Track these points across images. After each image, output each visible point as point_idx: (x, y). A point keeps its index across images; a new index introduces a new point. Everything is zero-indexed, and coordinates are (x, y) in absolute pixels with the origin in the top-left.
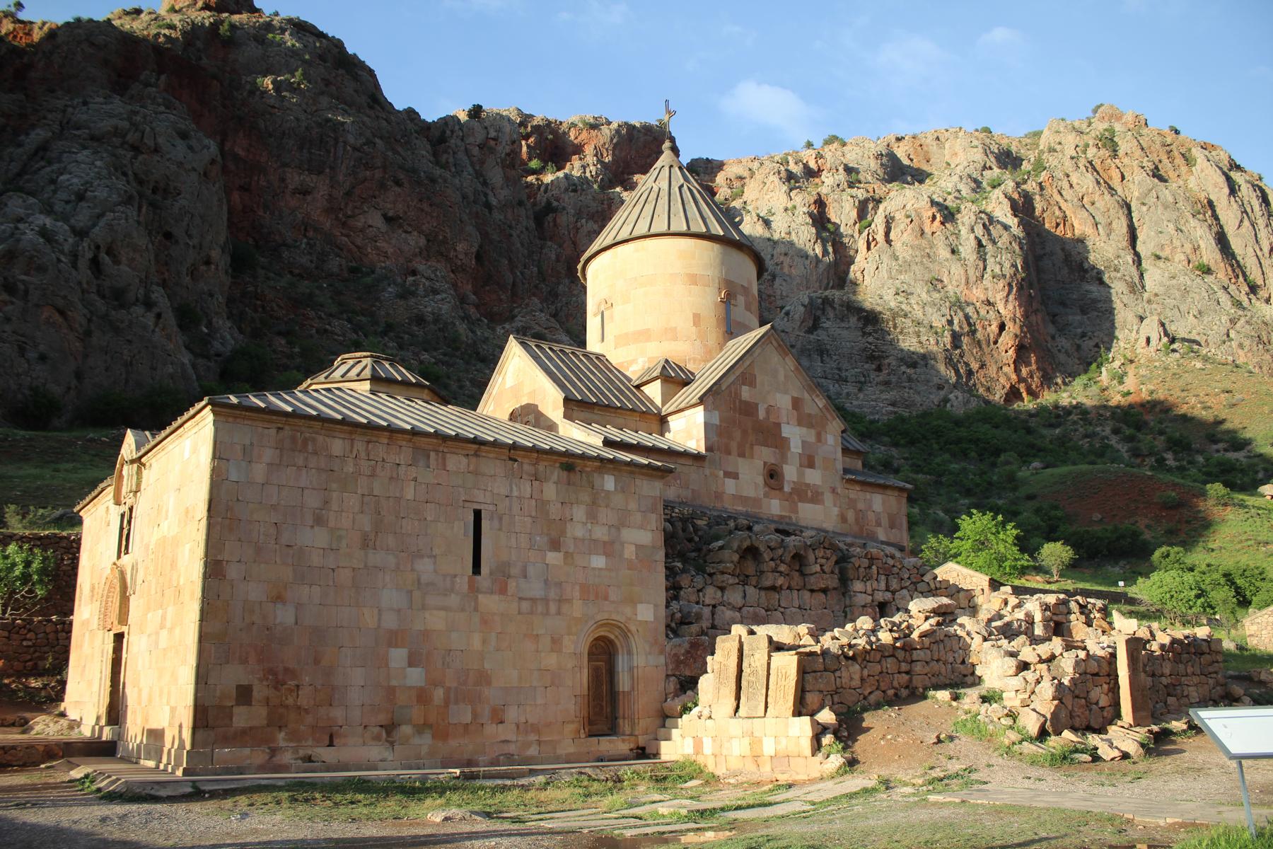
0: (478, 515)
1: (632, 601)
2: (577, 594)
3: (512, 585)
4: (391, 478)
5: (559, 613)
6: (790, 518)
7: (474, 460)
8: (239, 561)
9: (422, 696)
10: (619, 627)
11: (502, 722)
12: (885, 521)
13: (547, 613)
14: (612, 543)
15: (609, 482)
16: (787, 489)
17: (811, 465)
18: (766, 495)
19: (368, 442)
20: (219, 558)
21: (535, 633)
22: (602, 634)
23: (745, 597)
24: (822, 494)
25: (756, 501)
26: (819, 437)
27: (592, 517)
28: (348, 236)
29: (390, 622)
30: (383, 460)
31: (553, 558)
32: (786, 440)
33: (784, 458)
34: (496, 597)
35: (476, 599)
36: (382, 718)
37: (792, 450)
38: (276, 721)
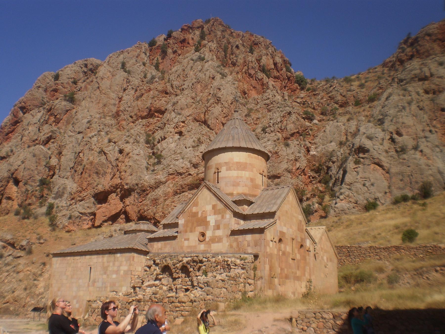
0: (91, 267)
1: (121, 286)
2: (109, 285)
3: (96, 284)
6: (208, 250)
12: (252, 244)
14: (118, 270)
15: (118, 255)
16: (207, 239)
17: (217, 227)
18: (199, 244)
24: (222, 239)
25: (195, 247)
26: (223, 217)
27: (114, 264)
31: (105, 276)
32: (209, 222)
33: (207, 229)
37: (211, 225)
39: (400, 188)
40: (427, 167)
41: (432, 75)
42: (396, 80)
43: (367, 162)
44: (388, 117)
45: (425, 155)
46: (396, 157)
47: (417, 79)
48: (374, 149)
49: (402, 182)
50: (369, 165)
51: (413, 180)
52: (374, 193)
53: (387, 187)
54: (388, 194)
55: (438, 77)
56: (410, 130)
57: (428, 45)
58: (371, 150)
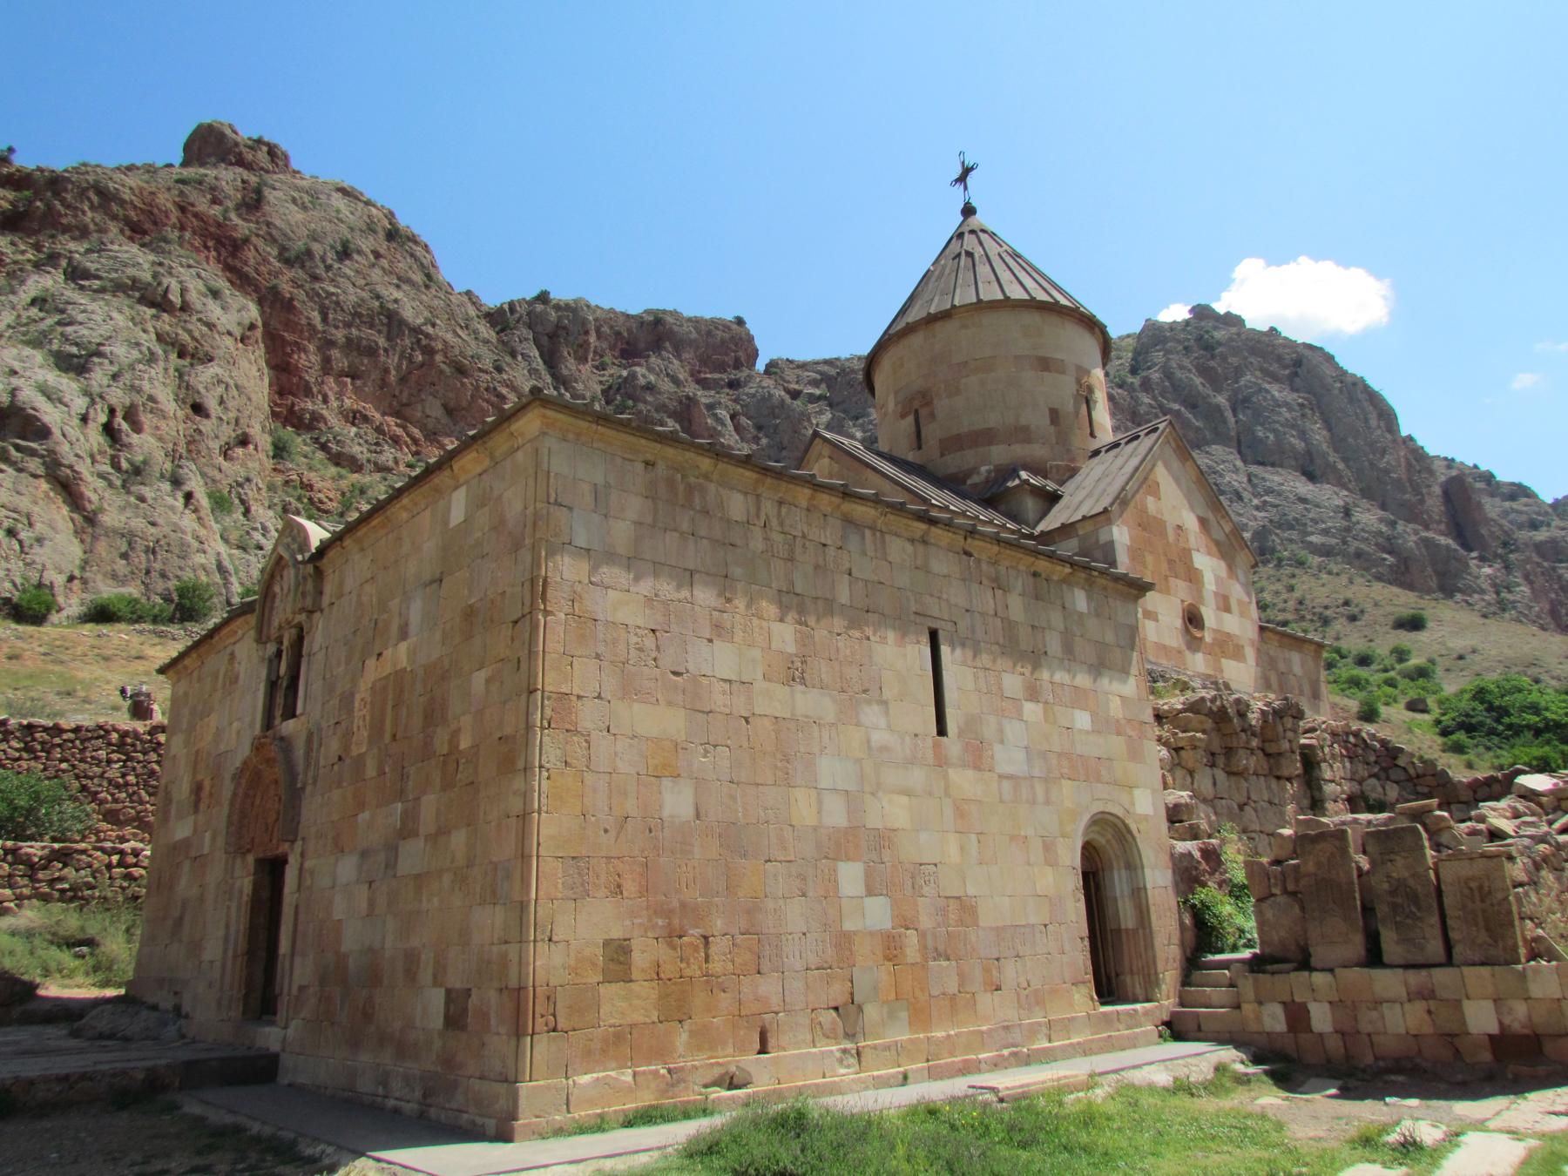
4: (817, 567)
5: (1047, 802)
7: (921, 548)
8: (599, 697)
9: (891, 948)
10: (1115, 825)
11: (998, 988)
12: (1307, 689)
13: (1034, 802)
16: (1208, 637)
19: (781, 503)
20: (564, 689)
21: (1023, 833)
22: (1091, 836)
23: (1215, 784)
28: (404, 428)
29: (836, 815)
30: (804, 537)
31: (1031, 710)
34: (970, 773)
35: (946, 776)
36: (837, 993)
38: (675, 1007)
39: (114, 576)
40: (195, 544)
41: (185, 307)
42: (64, 263)
43: (34, 465)
44: (106, 361)
45: (196, 511)
46: (118, 483)
47: (137, 294)
48: (64, 435)
49: (124, 562)
50: (35, 476)
51: (158, 566)
52: (40, 567)
53: (78, 562)
54: (76, 582)
55: (200, 320)
56: (162, 424)
57: (89, 214)
58: (57, 432)
